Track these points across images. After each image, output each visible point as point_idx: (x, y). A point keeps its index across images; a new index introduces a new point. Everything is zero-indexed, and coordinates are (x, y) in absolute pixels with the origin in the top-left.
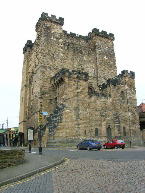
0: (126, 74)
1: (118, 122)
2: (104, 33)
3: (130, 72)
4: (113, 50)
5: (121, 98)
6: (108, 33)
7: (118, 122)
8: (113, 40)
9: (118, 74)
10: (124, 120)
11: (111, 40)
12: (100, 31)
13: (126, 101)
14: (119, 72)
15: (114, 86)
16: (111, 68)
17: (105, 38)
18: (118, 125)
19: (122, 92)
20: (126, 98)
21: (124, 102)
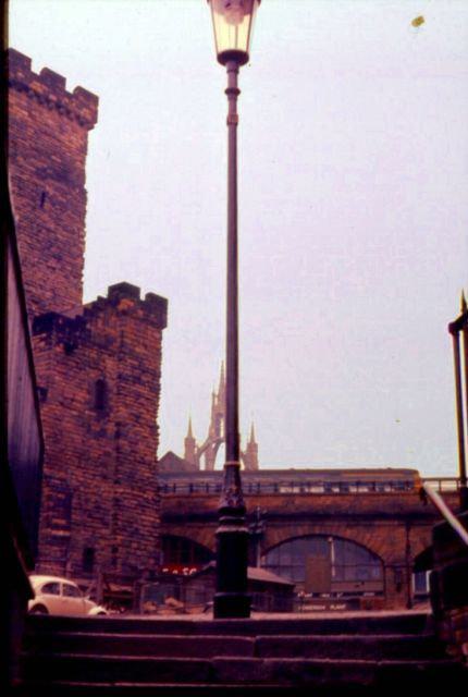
0: (125, 304)
1: (63, 522)
2: (52, 79)
3: (151, 296)
4: (82, 176)
5: (91, 410)
6: (70, 88)
7: (63, 522)
8: (88, 123)
9: (88, 298)
10: (90, 516)
11: (82, 124)
12: (36, 69)
13: (111, 428)
14: (93, 288)
15: (69, 350)
16: (59, 259)
17: (50, 109)
18: (61, 533)
19: (101, 387)
20: (112, 415)
21: (102, 434)
